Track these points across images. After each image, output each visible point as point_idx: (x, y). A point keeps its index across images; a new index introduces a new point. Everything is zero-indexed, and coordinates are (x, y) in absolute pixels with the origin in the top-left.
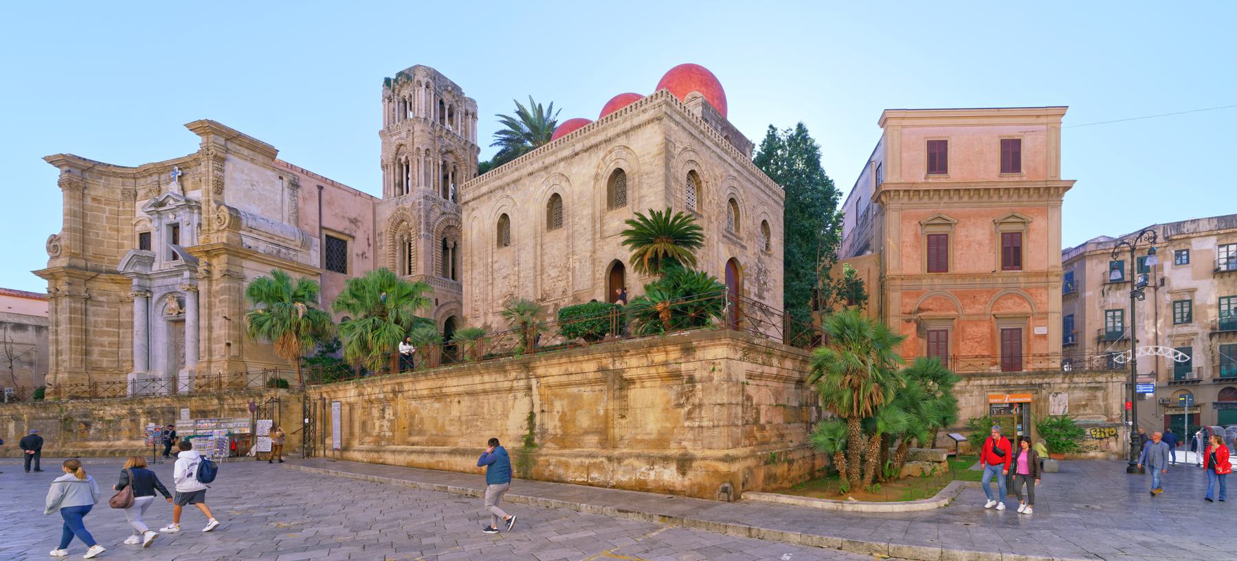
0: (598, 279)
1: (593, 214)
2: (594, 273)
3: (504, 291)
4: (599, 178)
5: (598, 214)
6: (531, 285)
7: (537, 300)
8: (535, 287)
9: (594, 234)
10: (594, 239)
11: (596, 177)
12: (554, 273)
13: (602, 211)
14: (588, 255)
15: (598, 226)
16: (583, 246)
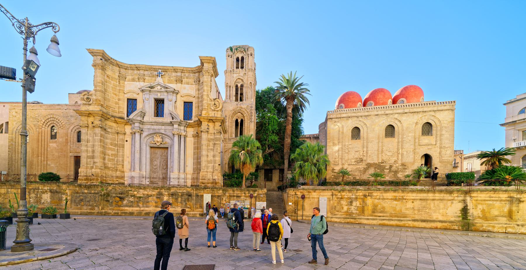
0: (417, 159)
1: (415, 136)
2: (414, 157)
3: (356, 156)
4: (418, 124)
5: (417, 136)
6: (376, 157)
7: (379, 163)
8: (378, 157)
9: (415, 143)
10: (415, 145)
11: (417, 123)
12: (389, 154)
13: (419, 136)
14: (412, 150)
15: (417, 140)
16: (409, 146)
